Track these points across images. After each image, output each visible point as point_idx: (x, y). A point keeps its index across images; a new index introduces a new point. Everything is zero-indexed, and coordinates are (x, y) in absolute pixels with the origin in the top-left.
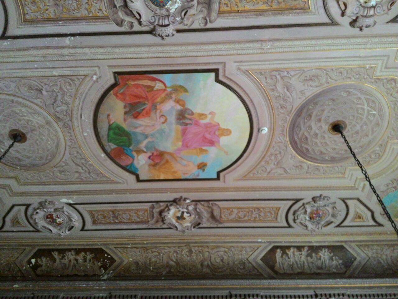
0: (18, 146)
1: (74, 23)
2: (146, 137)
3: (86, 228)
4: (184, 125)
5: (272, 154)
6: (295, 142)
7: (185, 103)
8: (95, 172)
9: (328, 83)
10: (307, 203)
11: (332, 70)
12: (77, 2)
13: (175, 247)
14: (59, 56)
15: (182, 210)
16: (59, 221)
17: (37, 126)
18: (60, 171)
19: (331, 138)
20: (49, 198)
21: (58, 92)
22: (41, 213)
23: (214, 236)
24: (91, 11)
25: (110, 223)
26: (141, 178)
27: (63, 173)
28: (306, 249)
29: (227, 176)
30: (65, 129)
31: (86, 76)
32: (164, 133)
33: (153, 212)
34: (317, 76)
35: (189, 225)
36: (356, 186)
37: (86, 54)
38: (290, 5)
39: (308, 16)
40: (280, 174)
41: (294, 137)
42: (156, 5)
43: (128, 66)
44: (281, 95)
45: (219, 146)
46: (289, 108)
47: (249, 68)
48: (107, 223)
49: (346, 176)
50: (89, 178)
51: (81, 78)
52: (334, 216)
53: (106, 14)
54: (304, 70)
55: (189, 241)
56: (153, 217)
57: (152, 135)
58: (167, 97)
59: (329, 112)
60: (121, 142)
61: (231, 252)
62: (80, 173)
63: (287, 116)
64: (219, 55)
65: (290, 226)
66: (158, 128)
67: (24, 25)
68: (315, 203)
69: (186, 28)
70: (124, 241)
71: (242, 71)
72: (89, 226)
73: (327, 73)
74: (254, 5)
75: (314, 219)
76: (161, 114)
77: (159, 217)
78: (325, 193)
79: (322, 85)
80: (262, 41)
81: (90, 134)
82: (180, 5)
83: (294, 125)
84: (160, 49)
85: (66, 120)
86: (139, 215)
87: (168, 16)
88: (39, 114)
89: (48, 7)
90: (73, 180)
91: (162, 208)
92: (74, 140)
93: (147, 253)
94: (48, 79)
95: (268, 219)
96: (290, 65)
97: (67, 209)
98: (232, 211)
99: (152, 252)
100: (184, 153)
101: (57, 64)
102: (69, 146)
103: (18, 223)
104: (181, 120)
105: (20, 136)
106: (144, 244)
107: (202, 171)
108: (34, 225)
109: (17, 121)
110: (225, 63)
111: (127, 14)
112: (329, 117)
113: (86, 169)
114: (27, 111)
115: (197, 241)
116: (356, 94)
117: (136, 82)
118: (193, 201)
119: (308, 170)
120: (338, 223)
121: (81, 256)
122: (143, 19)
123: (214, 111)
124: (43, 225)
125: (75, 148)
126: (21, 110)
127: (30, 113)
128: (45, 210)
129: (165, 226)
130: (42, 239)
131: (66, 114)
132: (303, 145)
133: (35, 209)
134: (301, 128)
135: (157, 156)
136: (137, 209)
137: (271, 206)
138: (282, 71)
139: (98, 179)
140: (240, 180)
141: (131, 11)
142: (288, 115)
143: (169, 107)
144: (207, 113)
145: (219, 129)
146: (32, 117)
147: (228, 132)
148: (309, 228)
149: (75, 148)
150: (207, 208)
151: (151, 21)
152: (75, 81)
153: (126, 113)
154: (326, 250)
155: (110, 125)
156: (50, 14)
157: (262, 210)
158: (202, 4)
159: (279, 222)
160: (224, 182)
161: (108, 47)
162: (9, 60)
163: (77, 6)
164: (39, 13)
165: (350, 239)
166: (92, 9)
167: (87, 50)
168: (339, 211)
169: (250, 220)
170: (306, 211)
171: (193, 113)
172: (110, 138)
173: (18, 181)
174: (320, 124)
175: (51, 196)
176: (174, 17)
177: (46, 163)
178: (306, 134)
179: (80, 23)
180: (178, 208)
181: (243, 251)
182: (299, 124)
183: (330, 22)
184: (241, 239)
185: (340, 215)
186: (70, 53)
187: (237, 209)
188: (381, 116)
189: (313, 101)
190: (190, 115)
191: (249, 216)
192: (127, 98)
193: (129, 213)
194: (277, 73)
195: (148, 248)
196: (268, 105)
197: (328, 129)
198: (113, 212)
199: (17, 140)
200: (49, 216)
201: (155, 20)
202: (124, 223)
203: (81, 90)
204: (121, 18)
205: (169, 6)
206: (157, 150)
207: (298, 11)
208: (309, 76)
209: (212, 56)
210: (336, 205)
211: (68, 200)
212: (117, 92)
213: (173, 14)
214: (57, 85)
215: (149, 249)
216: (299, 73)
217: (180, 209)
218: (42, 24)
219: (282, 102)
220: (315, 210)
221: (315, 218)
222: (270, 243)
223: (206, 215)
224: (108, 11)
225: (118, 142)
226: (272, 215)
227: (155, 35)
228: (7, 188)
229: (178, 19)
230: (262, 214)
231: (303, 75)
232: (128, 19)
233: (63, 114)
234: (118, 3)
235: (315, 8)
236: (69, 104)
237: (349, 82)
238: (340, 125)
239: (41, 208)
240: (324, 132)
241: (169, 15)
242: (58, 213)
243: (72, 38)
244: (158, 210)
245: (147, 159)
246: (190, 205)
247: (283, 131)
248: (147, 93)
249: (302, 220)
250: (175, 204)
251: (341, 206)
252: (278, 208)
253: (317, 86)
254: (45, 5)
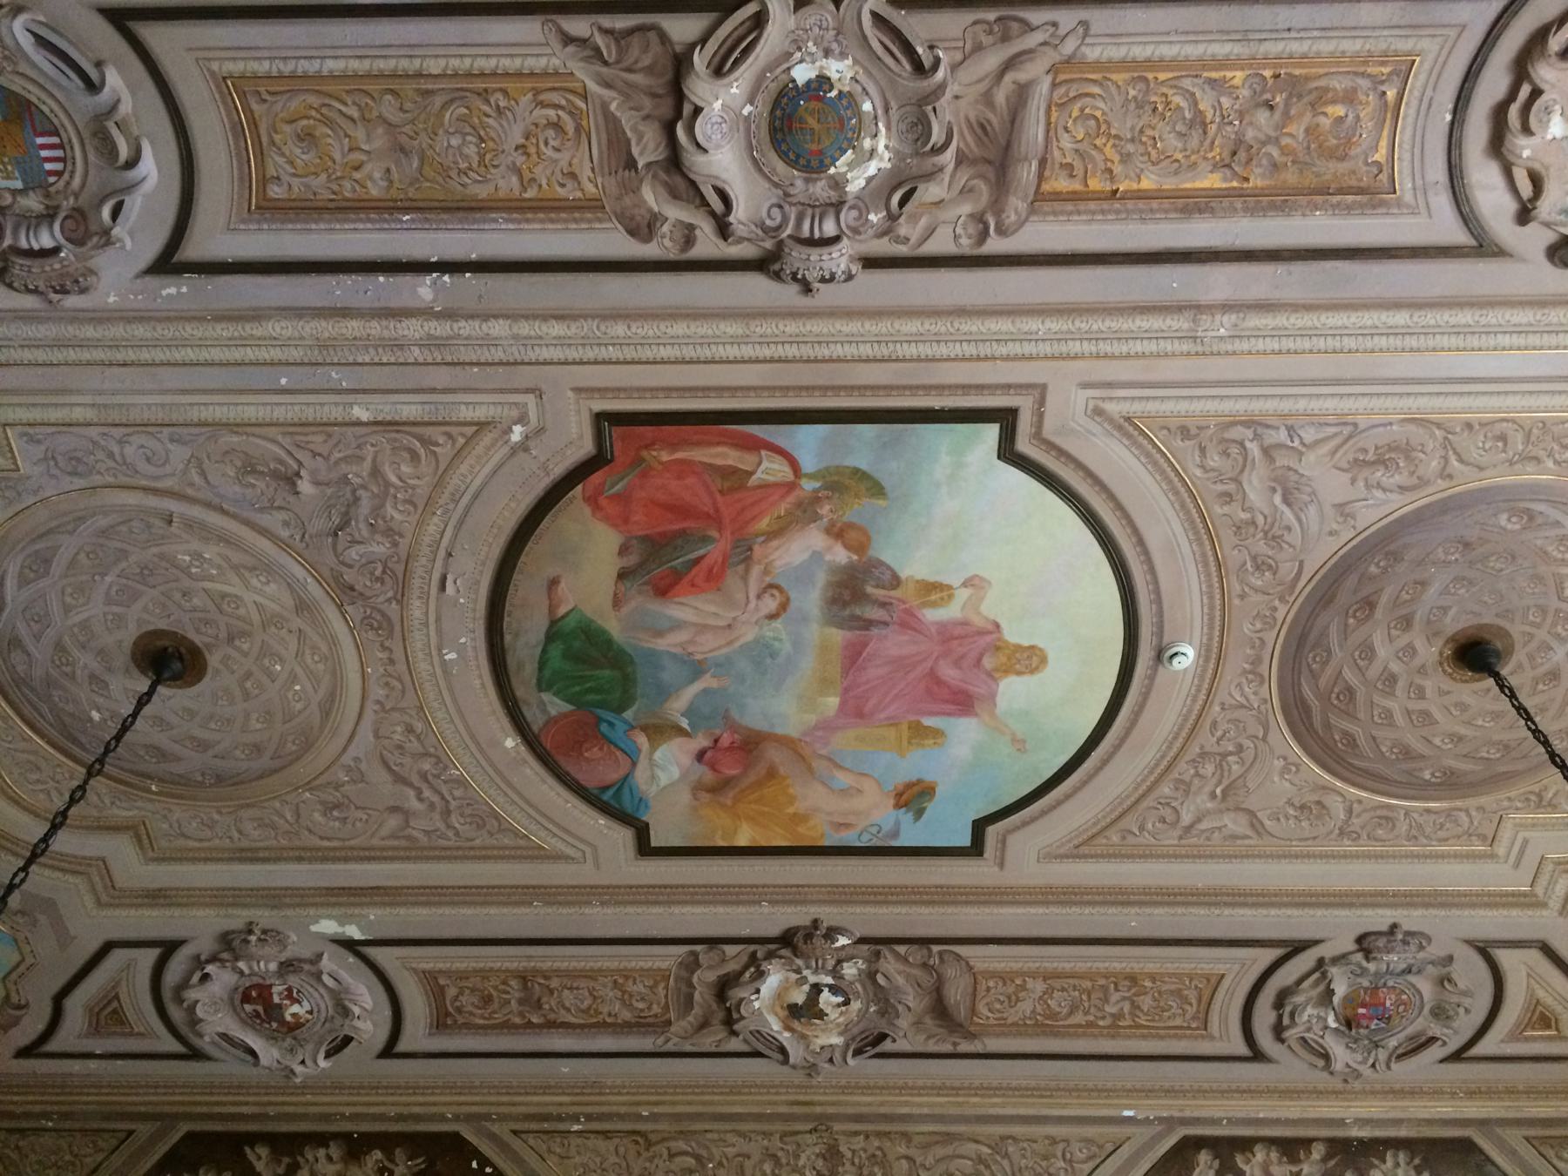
0: (169, 698)
1: (461, 222)
2: (697, 669)
3: (402, 1047)
4: (860, 629)
5: (1204, 755)
6: (1305, 708)
7: (869, 538)
8: (468, 811)
9: (1450, 477)
10: (1336, 960)
11: (1469, 426)
12: (482, 140)
13: (767, 1135)
14: (384, 347)
15: (813, 979)
16: (294, 1015)
17: (256, 618)
18: (322, 803)
20: (264, 917)
21: (364, 487)
22: (223, 979)
23: (940, 1090)
24: (533, 180)
25: (506, 1027)
26: (655, 842)
27: (335, 813)
28: (1318, 1152)
29: (1013, 840)
30: (371, 635)
31: (482, 426)
32: (773, 655)
33: (691, 985)
34: (1406, 450)
35: (837, 1040)
36: (1539, 890)
37: (490, 342)
38: (1318, 175)
39: (1389, 220)
40: (1234, 837)
41: (1300, 684)
42: (793, 164)
43: (654, 391)
44: (1260, 520)
45: (993, 715)
46: (1287, 570)
47: (1136, 408)
48: (494, 1027)
49: (1501, 850)
50: (443, 836)
51: (463, 435)
52: (1439, 1013)
53: (594, 190)
54: (1355, 425)
55: (831, 1110)
56: (688, 1003)
57: (718, 665)
58: (799, 513)
59: (1445, 591)
60: (589, 691)
61: (1005, 1163)
62: (407, 814)
63: (1277, 603)
64: (1023, 358)
65: (1257, 1056)
66: (750, 637)
67: (259, 222)
68: (1367, 959)
69: (902, 250)
70: (561, 1104)
71: (1111, 421)
72: (416, 1035)
73: (1446, 438)
74: (1176, 173)
75: (1359, 1026)
76: (768, 579)
77: (715, 1006)
78: (1411, 919)
79: (1423, 482)
80: (1198, 308)
81: (470, 653)
82: (887, 165)
83: (1303, 638)
84: (791, 327)
85: (381, 599)
86: (631, 996)
87: (838, 206)
88: (268, 569)
89: (364, 157)
90: (375, 842)
91: (733, 966)
92: (400, 680)
93: (651, 1159)
94: (330, 436)
95: (1171, 1024)
96: (1302, 405)
97: (335, 964)
98: (1023, 987)
99: (672, 1156)
100: (844, 742)
101: (372, 378)
102: (378, 702)
103: (118, 1017)
104: (845, 604)
105: (181, 658)
106: (639, 1117)
107: (910, 816)
108: (184, 1030)
109: (177, 596)
110: (1042, 389)
111: (675, 195)
112: (1445, 610)
113: (436, 799)
114: (227, 559)
115: (865, 1110)
116: (1558, 524)
117: (679, 455)
118: (862, 941)
119: (1346, 822)
120: (1453, 1046)
121: (370, 1165)
122: (740, 215)
123: (981, 573)
124: (221, 1030)
125: (402, 710)
126: (198, 556)
127: (236, 568)
128: (241, 965)
129: (735, 1045)
130: (210, 1088)
131: (384, 572)
132: (1333, 720)
133: (198, 962)
134: (1329, 652)
135: (731, 748)
136: (626, 969)
137: (1187, 967)
138: (1268, 426)
139: (478, 842)
140: (1067, 857)
141: (693, 184)
142: (1282, 599)
143: (804, 554)
144: (955, 581)
145: (998, 647)
146: (244, 585)
147: (1035, 660)
148: (1338, 1066)
149: (402, 710)
150: (916, 972)
151: (768, 222)
152: (437, 444)
153: (622, 575)
154: (1402, 1157)
155: (553, 623)
156: (369, 184)
157: (1148, 984)
158: (974, 162)
159: (1212, 1038)
160: (1001, 865)
161: (585, 317)
162: (178, 355)
163: (482, 157)
164: (324, 176)
165: (1503, 1114)
166: (538, 170)
167: (498, 328)
168: (1465, 994)
169: (1090, 1025)
170: (1330, 993)
171: (896, 582)
172: (547, 673)
173: (146, 841)
174: (1404, 640)
175: (274, 907)
176: (860, 210)
177: (276, 771)
178: (1349, 675)
179: (484, 221)
180: (798, 971)
181: (1055, 1156)
182: (1324, 634)
183: (1473, 243)
184: (1050, 1106)
185: (1467, 1011)
186: (430, 337)
187: (1045, 980)
189: (1385, 544)
190: (883, 588)
191: (1093, 1010)
192: (638, 517)
193: (592, 984)
194: (1249, 433)
195: (653, 1137)
196: (1204, 555)
197: (1436, 657)
198: (524, 978)
199: (166, 675)
200: (254, 994)
201: (785, 219)
202: (566, 1025)
203: (454, 481)
204: (650, 211)
205: (844, 169)
206: (733, 727)
207: (1350, 198)
208: (1377, 448)
209: (994, 358)
210: (1456, 971)
211: (342, 924)
212: (599, 492)
213: (857, 198)
214: (362, 459)
215: (658, 1143)
216: (1336, 435)
217: (806, 972)
218: (329, 222)
219: (1261, 547)
220: (1366, 989)
221: (1364, 1022)
222: (1170, 1123)
223: (913, 1000)
224: (599, 180)
225: (577, 688)
226: (1187, 1007)
227: (777, 276)
228: (93, 871)
229: (873, 217)
230: (1146, 1002)
231: (1351, 442)
232: (676, 213)
233: (372, 574)
234: (641, 154)
235: (1414, 189)
236: (401, 536)
237: (1530, 476)
238: (1488, 643)
239: (225, 956)
240: (1422, 671)
241: (843, 203)
242: (293, 980)
243: (446, 278)
244: (711, 976)
245: (687, 760)
246: (849, 959)
247: (1257, 661)
248: (718, 496)
249: (1309, 1030)
250: (784, 952)
251: (1471, 974)
252: (1214, 981)
253: (1402, 489)
254: (351, 150)
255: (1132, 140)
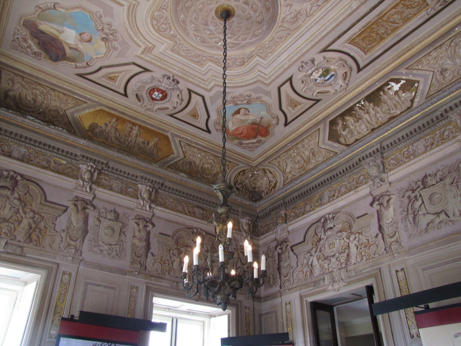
11: (289, 34)
19: (217, 3)
34: (293, 23)
39: (345, 39)
54: (308, 17)
116: (250, 39)
188: (212, 47)
253: (284, 18)
255: (403, 11)
